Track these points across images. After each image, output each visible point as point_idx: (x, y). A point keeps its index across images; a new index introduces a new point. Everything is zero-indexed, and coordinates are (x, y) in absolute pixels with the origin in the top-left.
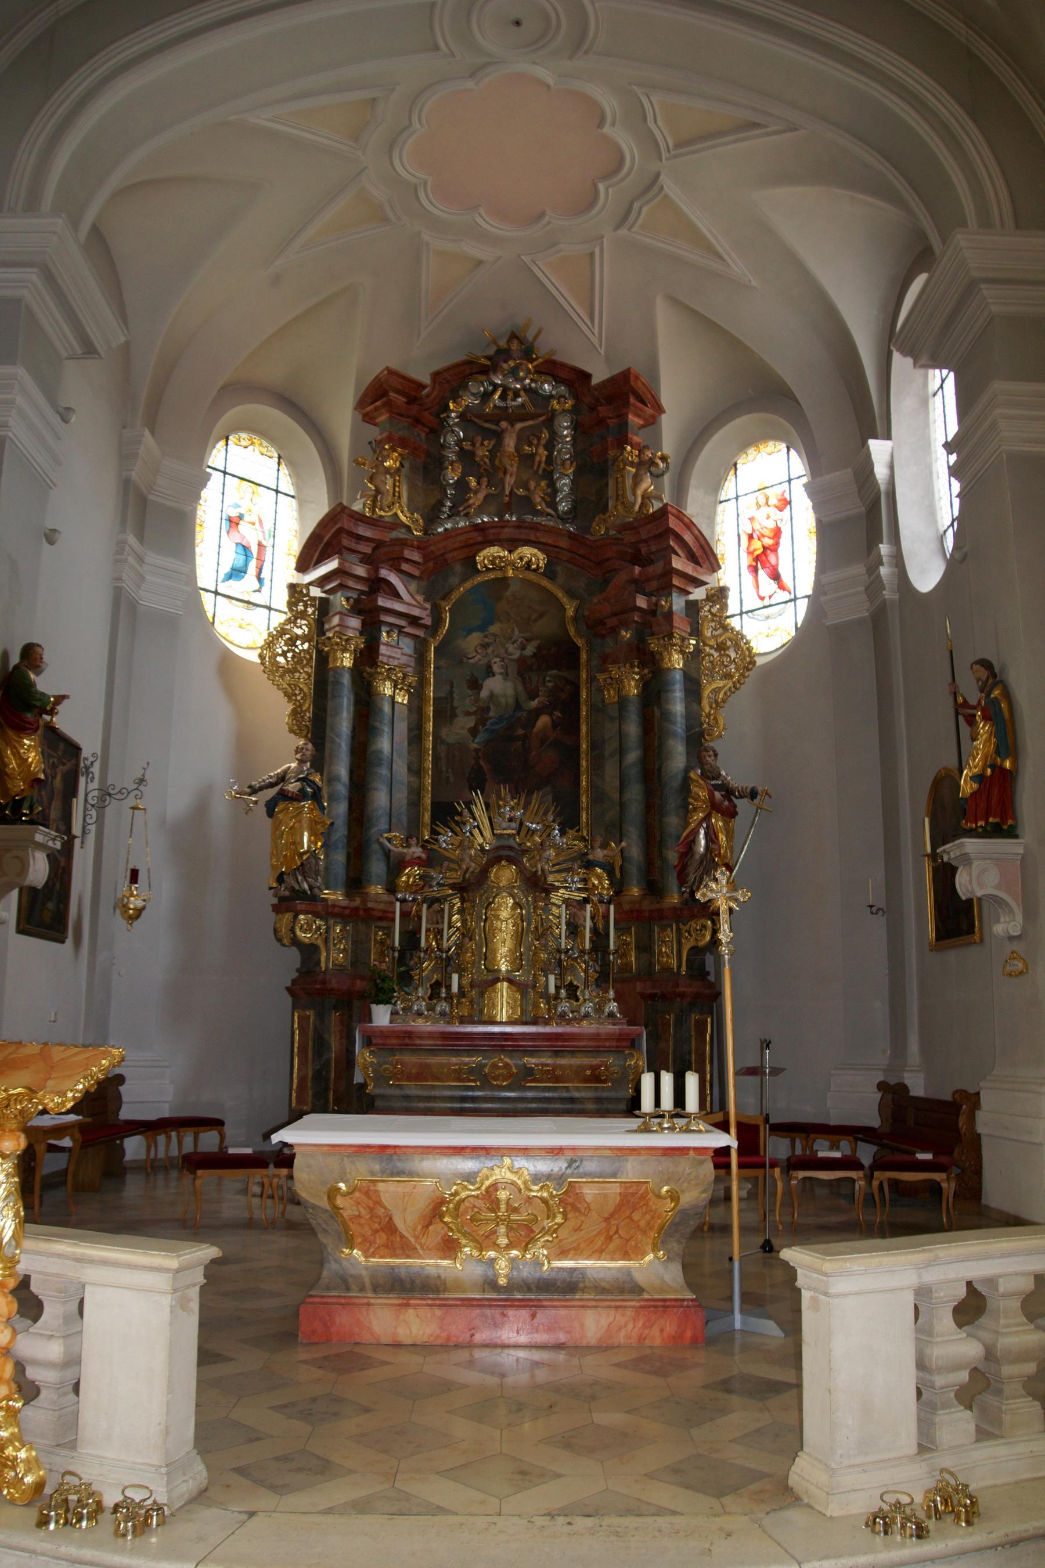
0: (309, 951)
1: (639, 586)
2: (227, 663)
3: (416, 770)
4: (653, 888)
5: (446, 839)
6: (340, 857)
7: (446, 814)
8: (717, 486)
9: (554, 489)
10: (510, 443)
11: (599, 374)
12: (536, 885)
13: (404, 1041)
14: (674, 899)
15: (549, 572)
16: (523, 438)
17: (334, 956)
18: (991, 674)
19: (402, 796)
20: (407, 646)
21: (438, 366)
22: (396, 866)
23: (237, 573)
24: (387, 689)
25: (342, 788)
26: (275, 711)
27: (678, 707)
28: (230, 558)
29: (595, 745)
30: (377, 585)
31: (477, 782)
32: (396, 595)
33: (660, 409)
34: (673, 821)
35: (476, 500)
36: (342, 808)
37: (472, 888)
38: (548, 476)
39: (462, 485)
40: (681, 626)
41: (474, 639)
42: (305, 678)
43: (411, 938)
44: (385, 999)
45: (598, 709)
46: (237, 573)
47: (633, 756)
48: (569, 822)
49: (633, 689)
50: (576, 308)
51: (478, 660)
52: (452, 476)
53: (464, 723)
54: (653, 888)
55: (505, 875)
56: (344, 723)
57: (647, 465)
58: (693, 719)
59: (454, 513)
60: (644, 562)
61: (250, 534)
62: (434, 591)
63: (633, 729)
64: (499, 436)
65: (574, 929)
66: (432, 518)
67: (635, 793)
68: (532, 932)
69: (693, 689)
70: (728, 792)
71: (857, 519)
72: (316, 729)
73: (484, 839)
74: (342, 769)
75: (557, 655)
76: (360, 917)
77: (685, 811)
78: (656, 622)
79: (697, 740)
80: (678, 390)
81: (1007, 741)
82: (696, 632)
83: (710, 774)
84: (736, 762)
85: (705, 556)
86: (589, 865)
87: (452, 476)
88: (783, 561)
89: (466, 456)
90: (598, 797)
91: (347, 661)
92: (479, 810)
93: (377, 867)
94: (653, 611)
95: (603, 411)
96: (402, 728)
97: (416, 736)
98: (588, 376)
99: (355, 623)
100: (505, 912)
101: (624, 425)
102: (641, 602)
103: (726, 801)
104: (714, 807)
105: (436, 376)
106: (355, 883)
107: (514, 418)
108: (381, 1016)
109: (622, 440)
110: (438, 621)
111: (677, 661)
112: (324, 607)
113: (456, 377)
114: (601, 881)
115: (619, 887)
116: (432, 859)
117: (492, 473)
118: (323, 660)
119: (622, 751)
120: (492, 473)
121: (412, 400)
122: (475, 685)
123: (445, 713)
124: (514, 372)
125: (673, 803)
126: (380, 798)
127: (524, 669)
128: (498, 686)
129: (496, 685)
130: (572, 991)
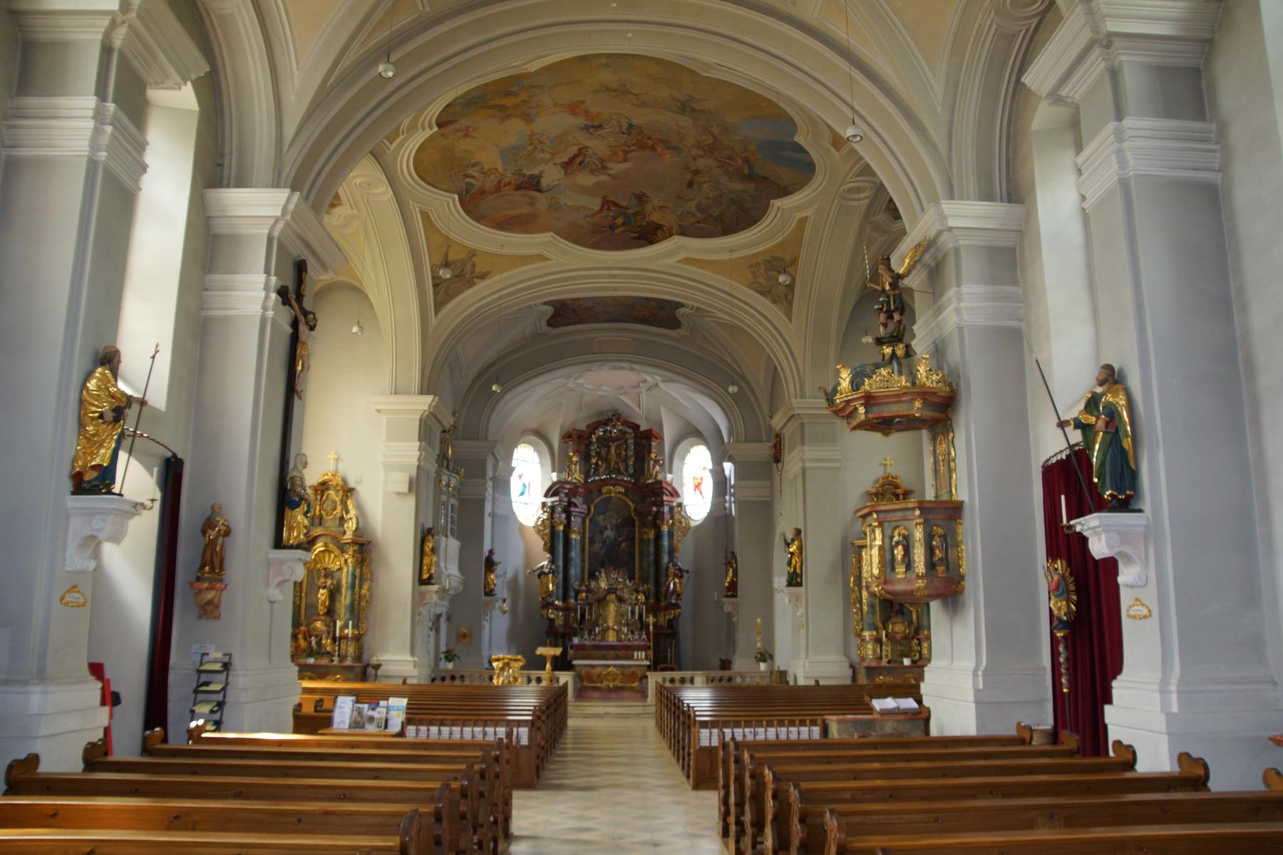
0: (552, 621)
1: (655, 504)
2: (521, 527)
3: (583, 561)
4: (658, 600)
5: (593, 584)
6: (561, 591)
7: (593, 576)
8: (683, 459)
9: (627, 466)
10: (613, 450)
11: (643, 428)
12: (621, 600)
13: (581, 647)
14: (663, 604)
15: (625, 494)
16: (617, 447)
17: (559, 623)
18: (733, 553)
19: (579, 569)
20: (579, 520)
21: (590, 421)
22: (578, 593)
23: (522, 494)
24: (574, 536)
25: (561, 569)
26: (538, 543)
27: (666, 543)
28: (520, 489)
29: (641, 552)
30: (570, 504)
31: (602, 565)
32: (576, 506)
33: (662, 439)
34: (663, 579)
35: (601, 470)
36: (561, 576)
37: (602, 601)
38: (626, 460)
39: (596, 464)
40: (667, 516)
41: (602, 517)
42: (547, 531)
43: (583, 616)
44: (575, 635)
45: (642, 540)
46: (522, 494)
47: (652, 558)
48: (632, 578)
49: (652, 536)
50: (635, 407)
51: (602, 524)
52: (594, 461)
53: (598, 546)
54: (658, 600)
55: (613, 596)
56: (561, 549)
57: (656, 462)
58: (670, 545)
59: (594, 474)
60: (653, 498)
61: (525, 480)
62: (588, 502)
63: (652, 549)
64: (609, 447)
65: (633, 612)
66: (587, 476)
67: (652, 570)
68: (620, 615)
69: (671, 534)
70: (680, 570)
71: (721, 484)
72: (551, 549)
73: (603, 585)
74: (561, 563)
75: (628, 522)
76: (566, 610)
77: (667, 576)
78: (659, 515)
79: (672, 552)
80: (668, 434)
81: (735, 574)
82: (672, 517)
83: (675, 565)
84: (685, 559)
85: (675, 494)
86: (638, 592)
87: (594, 461)
88: (703, 487)
89: (598, 454)
90: (641, 569)
91: (561, 528)
92: (603, 575)
93: (572, 594)
94: (658, 512)
95: (644, 442)
96: (578, 547)
97: (583, 550)
98: (638, 426)
99: (564, 516)
100: (612, 608)
101: (650, 445)
102: (655, 509)
103: (680, 573)
104: (676, 575)
105: (588, 426)
106: (565, 598)
107: (613, 440)
108: (576, 640)
109: (650, 452)
110: (589, 510)
111: (665, 528)
112: (553, 508)
113: (593, 427)
114: (641, 598)
115: (647, 598)
116: (589, 590)
117: (606, 460)
118: (553, 528)
119: (648, 555)
120: (606, 460)
121: (579, 437)
122: (602, 533)
123: (592, 542)
124: (614, 426)
125: (663, 573)
126: (573, 572)
127: (617, 528)
128: (609, 533)
129: (609, 533)
130: (632, 632)
